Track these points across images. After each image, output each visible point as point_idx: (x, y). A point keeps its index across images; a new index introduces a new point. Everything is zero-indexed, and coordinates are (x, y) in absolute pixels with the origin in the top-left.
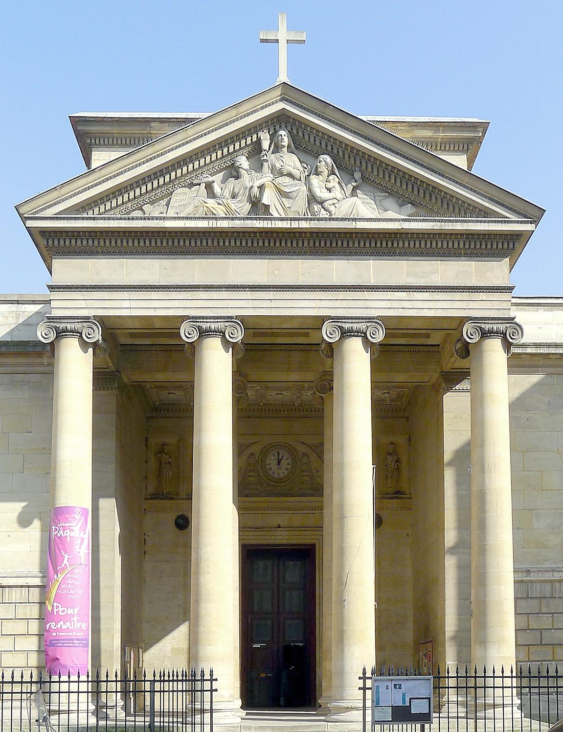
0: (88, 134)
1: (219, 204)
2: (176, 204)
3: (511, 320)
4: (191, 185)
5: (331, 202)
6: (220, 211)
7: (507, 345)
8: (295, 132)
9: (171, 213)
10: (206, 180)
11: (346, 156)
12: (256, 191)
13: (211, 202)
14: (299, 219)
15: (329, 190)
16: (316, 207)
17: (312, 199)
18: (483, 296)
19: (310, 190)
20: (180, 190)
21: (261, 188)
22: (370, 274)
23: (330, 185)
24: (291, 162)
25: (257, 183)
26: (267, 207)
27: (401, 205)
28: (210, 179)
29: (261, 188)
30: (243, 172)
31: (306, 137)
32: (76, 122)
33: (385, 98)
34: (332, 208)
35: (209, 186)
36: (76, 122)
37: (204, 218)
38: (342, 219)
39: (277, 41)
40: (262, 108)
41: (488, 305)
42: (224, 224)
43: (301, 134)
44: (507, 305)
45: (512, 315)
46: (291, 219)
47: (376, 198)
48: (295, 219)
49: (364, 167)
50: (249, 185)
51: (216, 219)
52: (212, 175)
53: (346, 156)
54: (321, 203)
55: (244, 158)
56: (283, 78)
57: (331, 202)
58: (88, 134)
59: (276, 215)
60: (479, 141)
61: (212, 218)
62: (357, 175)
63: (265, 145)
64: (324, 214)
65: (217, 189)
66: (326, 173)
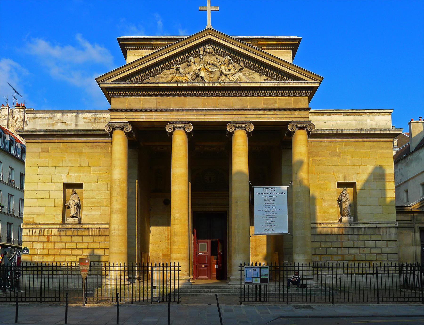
2: (163, 77)
4: (170, 69)
5: (230, 75)
9: (161, 80)
10: (177, 67)
12: (197, 70)
13: (178, 76)
14: (216, 83)
15: (229, 70)
16: (223, 77)
17: (222, 74)
18: (297, 112)
20: (165, 71)
21: (199, 70)
22: (247, 104)
23: (230, 68)
24: (212, 59)
25: (198, 68)
28: (178, 66)
30: (192, 63)
35: (177, 69)
37: (175, 83)
38: (235, 83)
39: (206, 10)
42: (184, 85)
45: (310, 120)
46: (213, 83)
48: (214, 83)
51: (181, 83)
52: (179, 65)
54: (226, 75)
55: (193, 58)
57: (230, 75)
59: (206, 81)
60: (297, 46)
61: (179, 83)
62: (242, 64)
63: (201, 53)
64: (227, 80)
65: (181, 70)
66: (228, 64)
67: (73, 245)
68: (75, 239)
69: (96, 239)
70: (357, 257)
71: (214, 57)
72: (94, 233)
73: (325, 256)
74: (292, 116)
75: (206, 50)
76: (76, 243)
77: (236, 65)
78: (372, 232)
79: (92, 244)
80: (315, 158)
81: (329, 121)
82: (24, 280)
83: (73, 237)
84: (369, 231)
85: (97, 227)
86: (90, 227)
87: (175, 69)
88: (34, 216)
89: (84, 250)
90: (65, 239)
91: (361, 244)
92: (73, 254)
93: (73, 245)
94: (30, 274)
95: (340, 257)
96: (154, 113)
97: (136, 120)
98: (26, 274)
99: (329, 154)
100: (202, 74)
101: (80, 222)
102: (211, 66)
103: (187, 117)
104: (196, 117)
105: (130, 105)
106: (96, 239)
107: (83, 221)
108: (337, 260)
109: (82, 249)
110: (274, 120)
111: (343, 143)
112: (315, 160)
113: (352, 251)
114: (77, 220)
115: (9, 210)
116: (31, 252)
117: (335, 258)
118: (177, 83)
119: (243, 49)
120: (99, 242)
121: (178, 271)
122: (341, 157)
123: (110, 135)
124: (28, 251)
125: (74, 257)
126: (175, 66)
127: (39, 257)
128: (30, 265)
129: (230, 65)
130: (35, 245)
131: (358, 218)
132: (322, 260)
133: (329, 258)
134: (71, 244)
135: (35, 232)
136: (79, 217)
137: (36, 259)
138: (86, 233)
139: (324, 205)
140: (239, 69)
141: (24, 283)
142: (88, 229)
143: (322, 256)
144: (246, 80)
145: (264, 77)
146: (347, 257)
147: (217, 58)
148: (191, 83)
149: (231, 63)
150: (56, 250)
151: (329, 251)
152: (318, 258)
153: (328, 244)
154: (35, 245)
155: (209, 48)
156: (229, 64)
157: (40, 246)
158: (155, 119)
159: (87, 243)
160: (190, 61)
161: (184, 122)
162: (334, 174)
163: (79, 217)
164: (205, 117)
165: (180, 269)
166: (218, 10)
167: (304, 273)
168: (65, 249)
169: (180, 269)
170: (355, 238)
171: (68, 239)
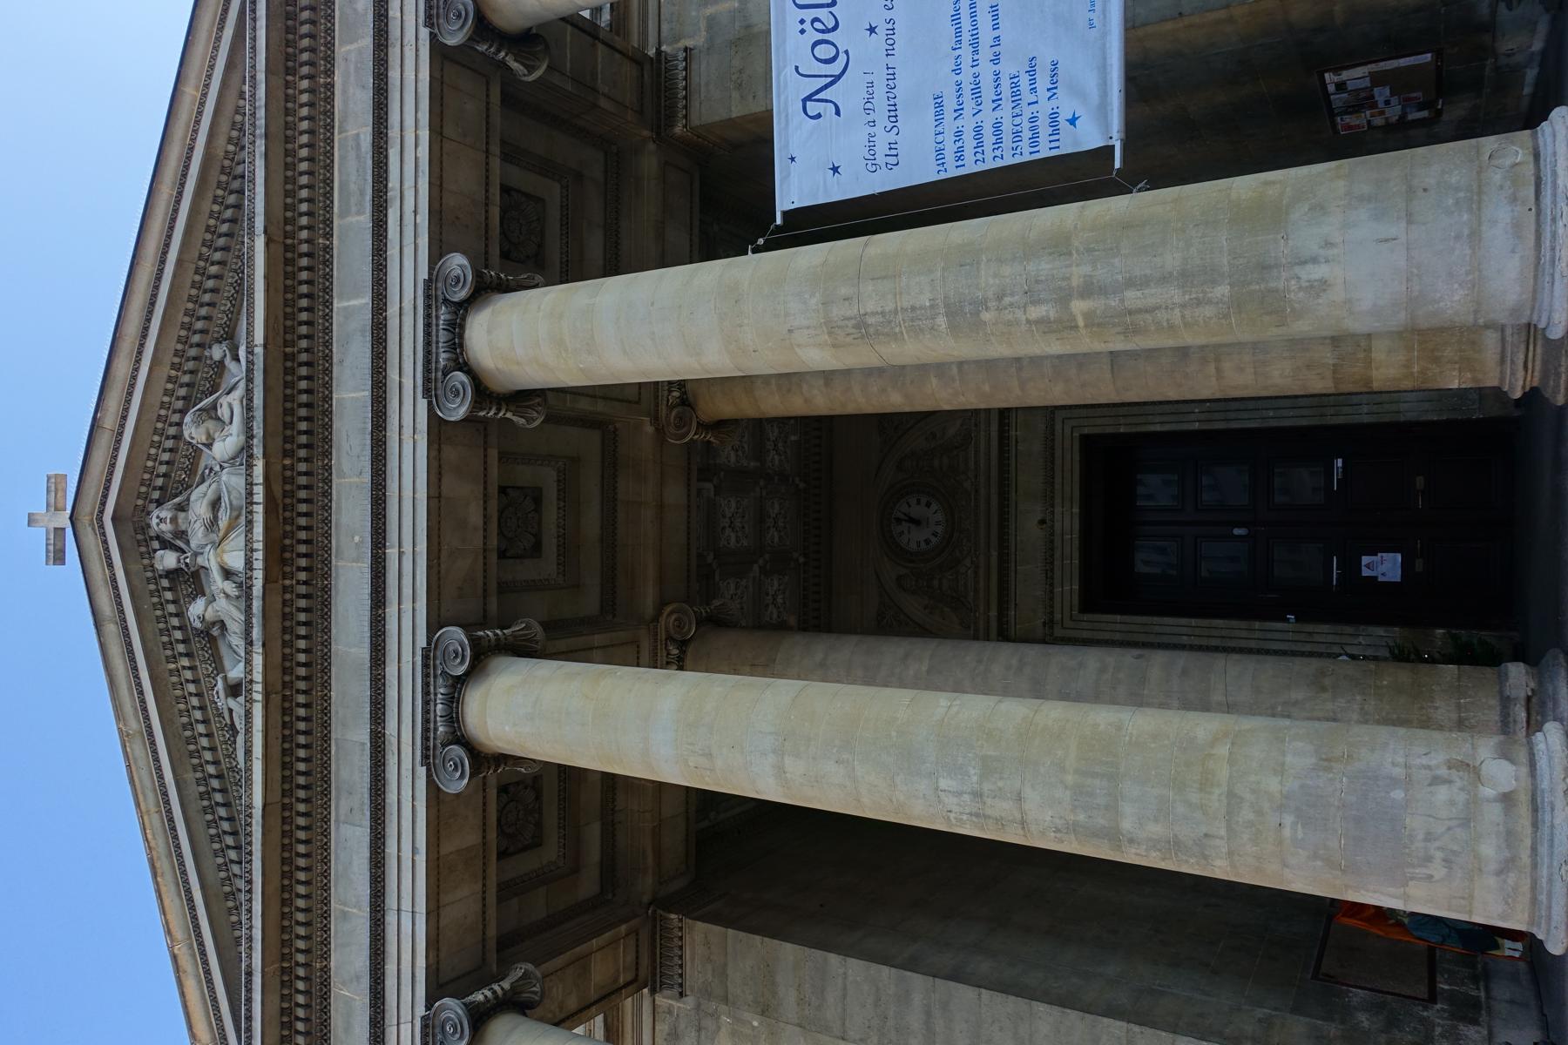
21: (227, 574)
24: (199, 507)
40: (110, 565)
66: (210, 424)
75: (168, 536)
87: (232, 703)
96: (391, 848)
104: (407, 606)
155: (160, 520)
158: (414, 850)
160: (203, 619)
164: (408, 548)
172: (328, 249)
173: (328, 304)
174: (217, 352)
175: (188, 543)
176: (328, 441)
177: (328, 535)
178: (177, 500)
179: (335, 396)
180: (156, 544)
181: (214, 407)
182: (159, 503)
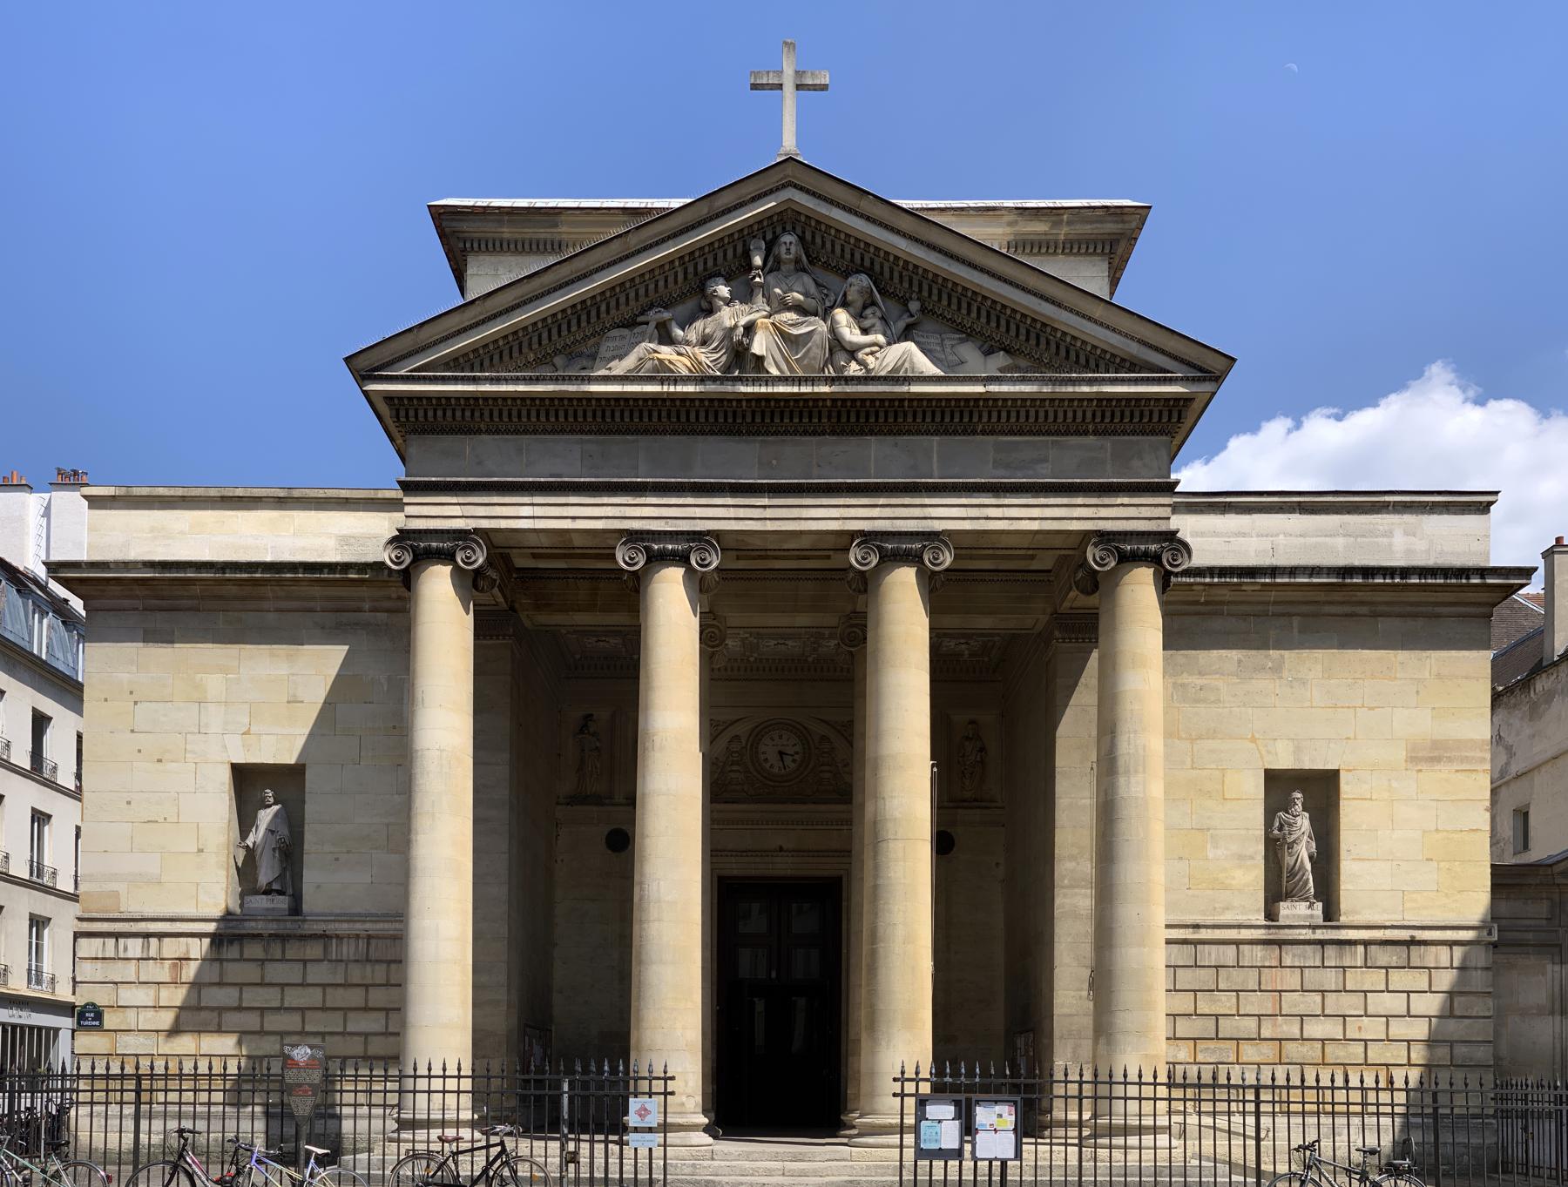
0: (461, 235)
1: (679, 354)
3: (1171, 536)
6: (682, 365)
7: (1164, 582)
8: (808, 236)
11: (896, 275)
13: (666, 352)
15: (865, 331)
17: (837, 344)
19: (833, 330)
20: (615, 332)
21: (750, 329)
23: (867, 323)
25: (743, 321)
26: (760, 359)
27: (988, 352)
29: (750, 329)
31: (828, 245)
32: (443, 218)
33: (958, 182)
34: (870, 360)
36: (443, 218)
39: (780, 86)
41: (1132, 512)
43: (818, 240)
44: (1166, 512)
47: (947, 342)
49: (925, 294)
50: (729, 323)
53: (896, 275)
56: (789, 143)
57: (868, 350)
58: (461, 235)
59: (774, 372)
62: (914, 306)
64: (853, 369)
66: (859, 304)
67: (270, 997)
68: (277, 972)
69: (356, 974)
70: (1335, 1053)
71: (807, 279)
72: (348, 950)
73: (1212, 1045)
74: (1104, 512)
75: (775, 250)
76: (371, 1005)
77: (893, 308)
78: (1394, 961)
79: (341, 991)
80: (1186, 679)
81: (1244, 535)
82: (84, 1123)
83: (269, 966)
84: (1383, 956)
85: (358, 927)
86: (331, 928)
87: (653, 325)
88: (121, 887)
89: (308, 1014)
90: (236, 972)
91: (1350, 1004)
92: (267, 1027)
93: (270, 997)
94: (107, 1103)
95: (1267, 1051)
97: (503, 524)
98: (92, 1103)
99: (1240, 661)
100: (759, 346)
101: (296, 909)
102: (791, 316)
103: (699, 512)
105: (479, 463)
106: (356, 974)
107: (306, 908)
108: (1257, 1059)
109: (302, 1010)
110: (1035, 526)
111: (1296, 621)
112: (1182, 685)
113: (1315, 1029)
114: (282, 903)
115: (37, 867)
116: (109, 1020)
117: (1250, 1052)
118: (662, 381)
119: (922, 243)
120: (367, 986)
121: (666, 1094)
122: (1285, 673)
123: (407, 579)
124: (99, 1016)
125: (272, 1038)
126: (654, 316)
127: (141, 1039)
128: (108, 1068)
129: (869, 311)
130: (128, 996)
131: (1343, 906)
132: (1200, 1058)
133: (1227, 1051)
134: (260, 990)
135: (126, 949)
136: (290, 891)
137: (130, 1044)
138: (314, 950)
139: (1210, 855)
140: (901, 325)
141: (83, 1137)
142: (324, 937)
143: (1201, 1045)
144: (931, 369)
145: (1001, 359)
146: (1293, 1050)
147: (818, 284)
148: (714, 379)
149: (874, 303)
150: (204, 1014)
151: (1226, 1027)
152: (1183, 1053)
153: (1226, 1003)
154: (128, 996)
156: (865, 307)
157: (142, 996)
159: (319, 990)
161: (688, 533)
162: (1253, 740)
163: (290, 891)
164: (769, 513)
165: (671, 1086)
166: (824, 87)
167: (1133, 1106)
168: (239, 1009)
169: (671, 1086)
170: (1330, 979)
171: (250, 972)
172: (974, 432)
173: (936, 433)
174: (914, 306)
175: (771, 271)
176: (842, 433)
177: (776, 433)
178: (804, 258)
179: (873, 438)
180: (769, 236)
181: (874, 303)
182: (802, 239)
